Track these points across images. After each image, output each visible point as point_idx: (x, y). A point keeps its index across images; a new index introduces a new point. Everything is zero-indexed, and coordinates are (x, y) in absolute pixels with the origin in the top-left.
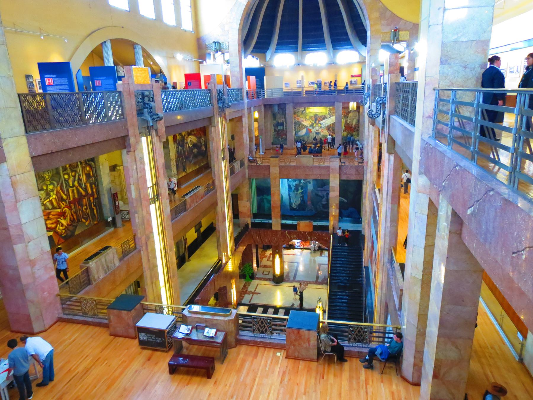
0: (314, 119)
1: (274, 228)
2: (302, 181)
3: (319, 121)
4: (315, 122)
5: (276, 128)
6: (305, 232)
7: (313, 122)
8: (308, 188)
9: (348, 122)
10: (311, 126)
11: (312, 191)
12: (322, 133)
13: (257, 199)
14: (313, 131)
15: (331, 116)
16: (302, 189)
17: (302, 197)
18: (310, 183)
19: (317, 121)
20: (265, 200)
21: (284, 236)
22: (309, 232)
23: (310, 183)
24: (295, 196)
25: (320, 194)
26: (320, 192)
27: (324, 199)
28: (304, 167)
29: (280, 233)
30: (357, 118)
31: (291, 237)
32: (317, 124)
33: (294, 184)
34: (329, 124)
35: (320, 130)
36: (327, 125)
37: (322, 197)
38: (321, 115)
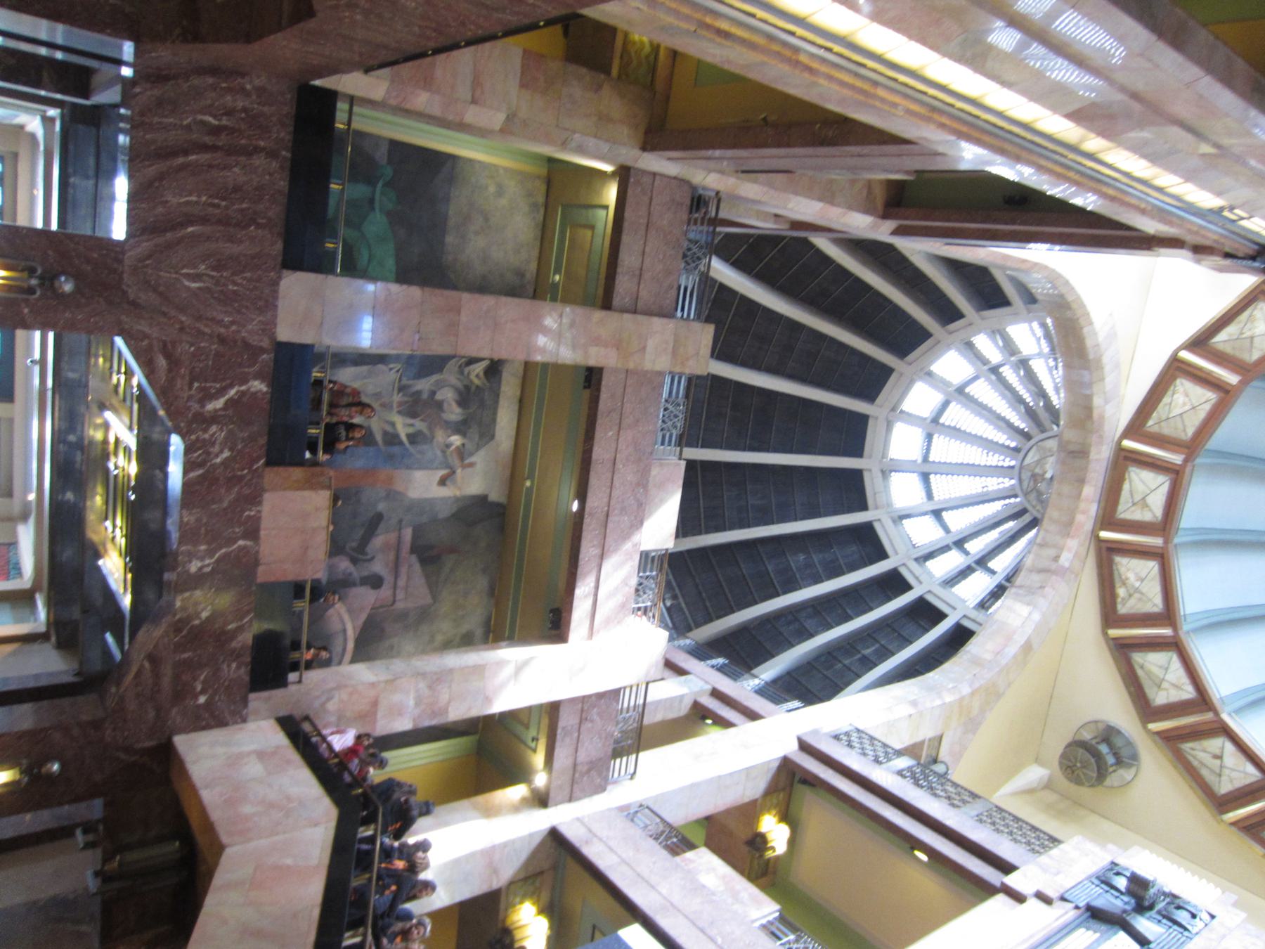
1: (295, 287)
2: (456, 440)
6: (253, 533)
13: (378, 138)
16: (413, 438)
18: (443, 482)
21: (228, 360)
22: (256, 563)
23: (443, 482)
25: (378, 541)
26: (392, 537)
29: (250, 331)
31: (214, 418)
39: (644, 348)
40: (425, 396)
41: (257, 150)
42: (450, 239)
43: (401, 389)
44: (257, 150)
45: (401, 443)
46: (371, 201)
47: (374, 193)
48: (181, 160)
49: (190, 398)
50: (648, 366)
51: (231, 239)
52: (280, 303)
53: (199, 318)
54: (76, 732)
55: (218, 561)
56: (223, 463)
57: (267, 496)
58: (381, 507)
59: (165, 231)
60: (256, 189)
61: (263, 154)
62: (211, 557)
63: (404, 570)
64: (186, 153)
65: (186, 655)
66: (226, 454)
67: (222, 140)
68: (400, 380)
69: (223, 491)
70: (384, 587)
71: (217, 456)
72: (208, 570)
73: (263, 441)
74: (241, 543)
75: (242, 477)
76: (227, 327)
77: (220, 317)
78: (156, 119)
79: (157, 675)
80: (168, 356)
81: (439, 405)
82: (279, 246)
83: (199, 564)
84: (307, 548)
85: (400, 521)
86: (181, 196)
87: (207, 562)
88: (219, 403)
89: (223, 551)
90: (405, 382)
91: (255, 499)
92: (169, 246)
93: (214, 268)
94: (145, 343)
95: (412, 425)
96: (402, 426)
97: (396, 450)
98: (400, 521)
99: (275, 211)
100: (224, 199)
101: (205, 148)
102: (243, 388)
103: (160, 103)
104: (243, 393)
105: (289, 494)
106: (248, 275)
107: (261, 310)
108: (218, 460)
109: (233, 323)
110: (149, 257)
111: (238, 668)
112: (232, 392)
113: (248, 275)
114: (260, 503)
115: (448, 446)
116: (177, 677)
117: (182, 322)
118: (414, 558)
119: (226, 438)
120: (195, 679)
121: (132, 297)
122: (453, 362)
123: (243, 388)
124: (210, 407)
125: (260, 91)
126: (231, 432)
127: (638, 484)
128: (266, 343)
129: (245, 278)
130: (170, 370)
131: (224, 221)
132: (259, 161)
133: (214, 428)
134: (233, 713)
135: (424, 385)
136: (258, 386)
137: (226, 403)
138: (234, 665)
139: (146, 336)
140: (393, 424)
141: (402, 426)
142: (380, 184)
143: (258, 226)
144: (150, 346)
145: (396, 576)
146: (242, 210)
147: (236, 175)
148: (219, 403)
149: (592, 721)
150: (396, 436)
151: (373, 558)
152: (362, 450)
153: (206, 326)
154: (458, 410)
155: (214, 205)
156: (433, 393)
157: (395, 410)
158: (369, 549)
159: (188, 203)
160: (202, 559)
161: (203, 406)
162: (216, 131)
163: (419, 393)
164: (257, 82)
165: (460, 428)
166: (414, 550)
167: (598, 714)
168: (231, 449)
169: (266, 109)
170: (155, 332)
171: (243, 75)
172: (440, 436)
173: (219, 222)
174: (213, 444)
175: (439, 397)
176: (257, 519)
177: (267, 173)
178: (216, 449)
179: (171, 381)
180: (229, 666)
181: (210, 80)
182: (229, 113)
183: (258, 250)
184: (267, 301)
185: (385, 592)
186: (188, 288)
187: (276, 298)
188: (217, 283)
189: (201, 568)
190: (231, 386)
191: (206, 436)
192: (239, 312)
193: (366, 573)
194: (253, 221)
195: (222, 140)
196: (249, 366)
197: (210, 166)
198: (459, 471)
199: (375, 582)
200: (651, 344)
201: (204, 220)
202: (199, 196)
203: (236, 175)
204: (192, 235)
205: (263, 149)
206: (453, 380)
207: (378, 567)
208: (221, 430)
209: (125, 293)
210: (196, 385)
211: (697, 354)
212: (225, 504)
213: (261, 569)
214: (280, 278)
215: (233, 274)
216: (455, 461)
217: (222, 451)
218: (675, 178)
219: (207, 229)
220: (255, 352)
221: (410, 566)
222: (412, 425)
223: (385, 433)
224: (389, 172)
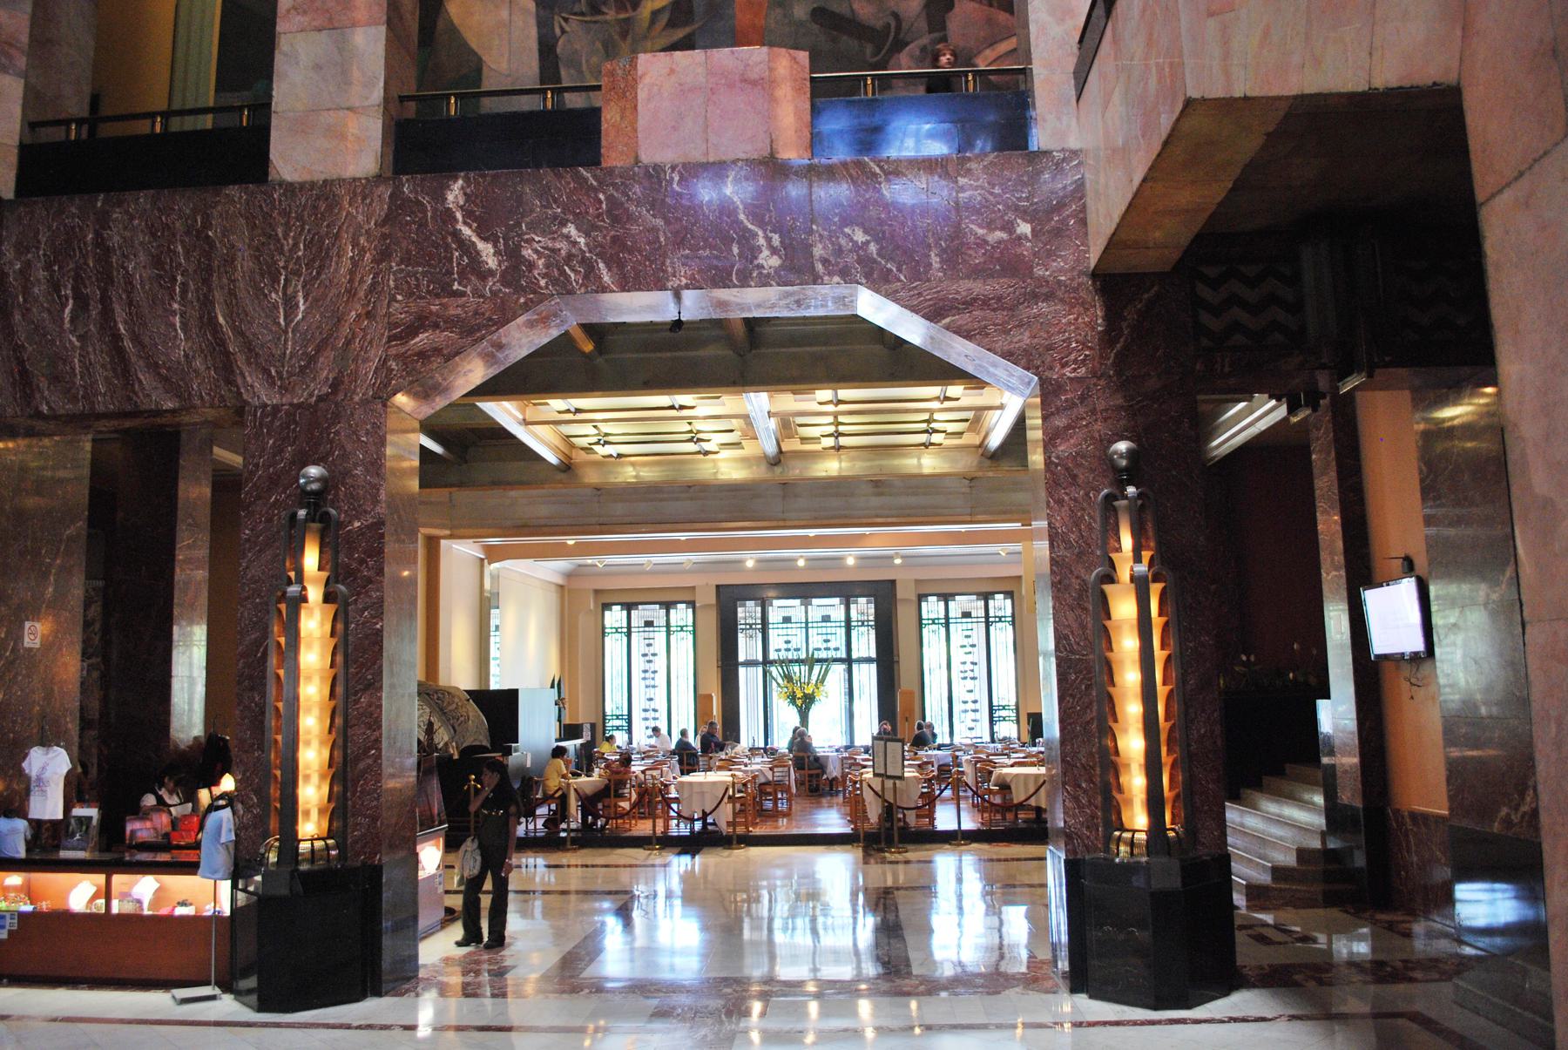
1: (290, 159)
29: (364, 216)
31: (512, 255)
41: (100, 241)
44: (100, 241)
48: (127, 344)
49: (477, 293)
51: (230, 261)
52: (320, 178)
53: (351, 293)
54: (1060, 422)
55: (761, 224)
56: (587, 235)
59: (227, 354)
60: (153, 235)
61: (105, 234)
64: (117, 337)
65: (935, 260)
66: (571, 229)
67: (93, 291)
68: (582, 14)
71: (575, 243)
73: (546, 174)
75: (610, 198)
76: (363, 251)
78: (78, 381)
79: (969, 303)
80: (412, 331)
82: (233, 191)
83: (766, 253)
86: (176, 337)
87: (762, 241)
88: (486, 250)
92: (249, 348)
93: (276, 280)
94: (393, 364)
99: (183, 204)
101: (107, 314)
102: (459, 216)
103: (55, 379)
104: (469, 215)
105: (642, 122)
107: (333, 203)
108: (582, 240)
109: (355, 244)
110: (267, 372)
112: (467, 231)
114: (658, 168)
116: (976, 273)
117: (359, 316)
119: (543, 234)
121: (326, 389)
124: (492, 263)
125: (21, 249)
126: (532, 227)
128: (385, 192)
129: (286, 236)
130: (436, 326)
131: (205, 274)
132: (115, 239)
133: (527, 252)
136: (455, 194)
139: (384, 362)
140: (655, 14)
143: (207, 224)
144: (397, 357)
147: (138, 267)
148: (486, 250)
151: (896, 16)
153: (362, 281)
155: (184, 291)
157: (630, 14)
158: (879, 24)
159: (184, 326)
161: (491, 273)
162: (82, 302)
168: (563, 224)
170: (376, 354)
173: (206, 282)
174: (555, 251)
177: (129, 224)
178: (563, 246)
179: (451, 323)
181: (18, 317)
182: (56, 287)
184: (318, 198)
186: (306, 313)
187: (313, 184)
188: (298, 273)
189: (774, 251)
190: (456, 234)
191: (541, 262)
192: (337, 236)
195: (93, 291)
196: (425, 211)
197: (130, 304)
201: (206, 303)
202: (174, 313)
203: (138, 267)
204: (230, 316)
205: (98, 234)
209: (320, 399)
210: (456, 286)
212: (659, 222)
214: (281, 183)
215: (281, 252)
217: (568, 237)
219: (218, 295)
223: (672, 24)
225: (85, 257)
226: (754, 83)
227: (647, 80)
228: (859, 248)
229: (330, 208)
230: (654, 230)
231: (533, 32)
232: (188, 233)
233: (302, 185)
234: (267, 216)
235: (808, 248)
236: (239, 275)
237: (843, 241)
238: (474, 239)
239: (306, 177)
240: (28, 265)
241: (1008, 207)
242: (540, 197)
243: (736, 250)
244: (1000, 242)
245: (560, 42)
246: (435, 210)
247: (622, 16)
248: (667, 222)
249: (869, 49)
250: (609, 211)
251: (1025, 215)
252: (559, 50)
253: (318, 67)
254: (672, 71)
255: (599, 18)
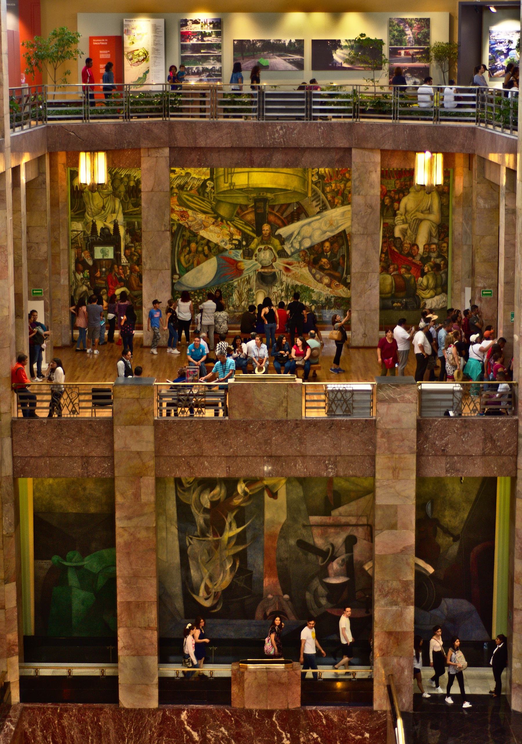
0: (250, 217)
2: (241, 488)
3: (274, 228)
4: (259, 232)
5: (85, 255)
6: (269, 713)
7: (248, 230)
8: (268, 515)
9: (397, 233)
10: (238, 246)
11: (285, 532)
12: (287, 279)
14: (250, 266)
15: (324, 208)
17: (241, 557)
18: (274, 495)
19: (266, 228)
20: (73, 579)
23: (274, 495)
24: (210, 553)
25: (319, 542)
26: (316, 531)
27: (335, 566)
28: (263, 426)
29: (155, 722)
30: (435, 217)
31: (203, 736)
32: (265, 241)
33: (206, 499)
34: (318, 238)
35: (280, 263)
36: (307, 244)
37: (328, 556)
38: (282, 200)
39: (139, 453)
40: (208, 516)
41: (60, 724)
42: (92, 510)
43: (203, 534)
44: (60, 724)
45: (244, 531)
46: (77, 568)
47: (71, 567)
50: (151, 448)
51: (108, 733)
52: (138, 707)
55: (284, 730)
56: (228, 731)
57: (247, 707)
58: (292, 542)
60: (80, 723)
61: (62, 721)
62: (282, 734)
63: (343, 520)
66: (223, 729)
68: (198, 536)
69: (243, 730)
70: (356, 534)
71: (224, 734)
72: (289, 735)
74: (274, 719)
75: (235, 720)
76: (153, 733)
77: (148, 737)
81: (214, 504)
83: (285, 739)
84: (280, 683)
85: (304, 526)
87: (284, 736)
88: (195, 735)
89: (278, 728)
90: (198, 533)
91: (249, 713)
95: (230, 524)
96: (232, 531)
97: (249, 535)
98: (304, 526)
100: (88, 738)
102: (186, 723)
104: (189, 723)
106: (125, 724)
108: (226, 733)
109: (151, 730)
111: (351, 717)
112: (188, 728)
113: (125, 724)
114: (251, 711)
115: (245, 493)
118: (335, 513)
119: (214, 730)
120: (354, 739)
122: (181, 497)
123: (186, 723)
125: (31, 725)
126: (210, 728)
127: (246, 431)
129: (127, 726)
132: (65, 723)
133: (209, 736)
134: (379, 718)
135: (200, 519)
137: (195, 731)
138: (348, 719)
140: (230, 539)
141: (232, 531)
142: (66, 563)
143: (98, 720)
145: (347, 525)
146: (92, 729)
148: (195, 735)
149: (447, 445)
150: (239, 535)
151: (332, 545)
152: (250, 560)
154: (217, 489)
156: (206, 511)
158: (324, 548)
160: (282, 739)
163: (205, 521)
164: (27, 726)
165: (231, 491)
166: (327, 513)
167: (442, 439)
168: (220, 727)
169: (39, 721)
171: (26, 733)
172: (237, 502)
174: (217, 736)
175: (208, 505)
176: (261, 712)
178: (220, 734)
180: (349, 722)
183: (111, 720)
184: (137, 714)
185: (360, 533)
187: (135, 710)
188: (132, 739)
189: (288, 739)
190: (185, 729)
191: (213, 739)
192: (145, 727)
193: (343, 549)
194: (96, 723)
196: (174, 721)
198: (265, 482)
199: (351, 541)
200: (135, 448)
205: (59, 721)
206: (194, 496)
207: (339, 540)
208: (209, 732)
211: (138, 399)
212: (251, 728)
213: (291, 707)
214: (124, 708)
216: (258, 485)
217: (222, 732)
218: (12, 437)
220: (165, 719)
221: (340, 515)
222: (230, 524)
223: (237, 544)
224: (56, 558)
225: (55, 728)
226: (283, 684)
227: (247, 681)
228: (314, 739)
229: (142, 717)
230: (250, 730)
231: (177, 543)
232: (92, 722)
233: (131, 710)
234: (120, 719)
235: (299, 739)
236: (111, 738)
237: (310, 737)
238: (191, 730)
239: (134, 707)
240: (34, 731)
241: (362, 728)
242: (212, 718)
243: (276, 738)
244: (359, 739)
245: (189, 548)
246: (177, 721)
247: (215, 539)
248: (254, 728)
249: (320, 559)
250: (235, 724)
251: (367, 731)
252: (188, 552)
253: (134, 669)
254: (256, 678)
255: (204, 539)
